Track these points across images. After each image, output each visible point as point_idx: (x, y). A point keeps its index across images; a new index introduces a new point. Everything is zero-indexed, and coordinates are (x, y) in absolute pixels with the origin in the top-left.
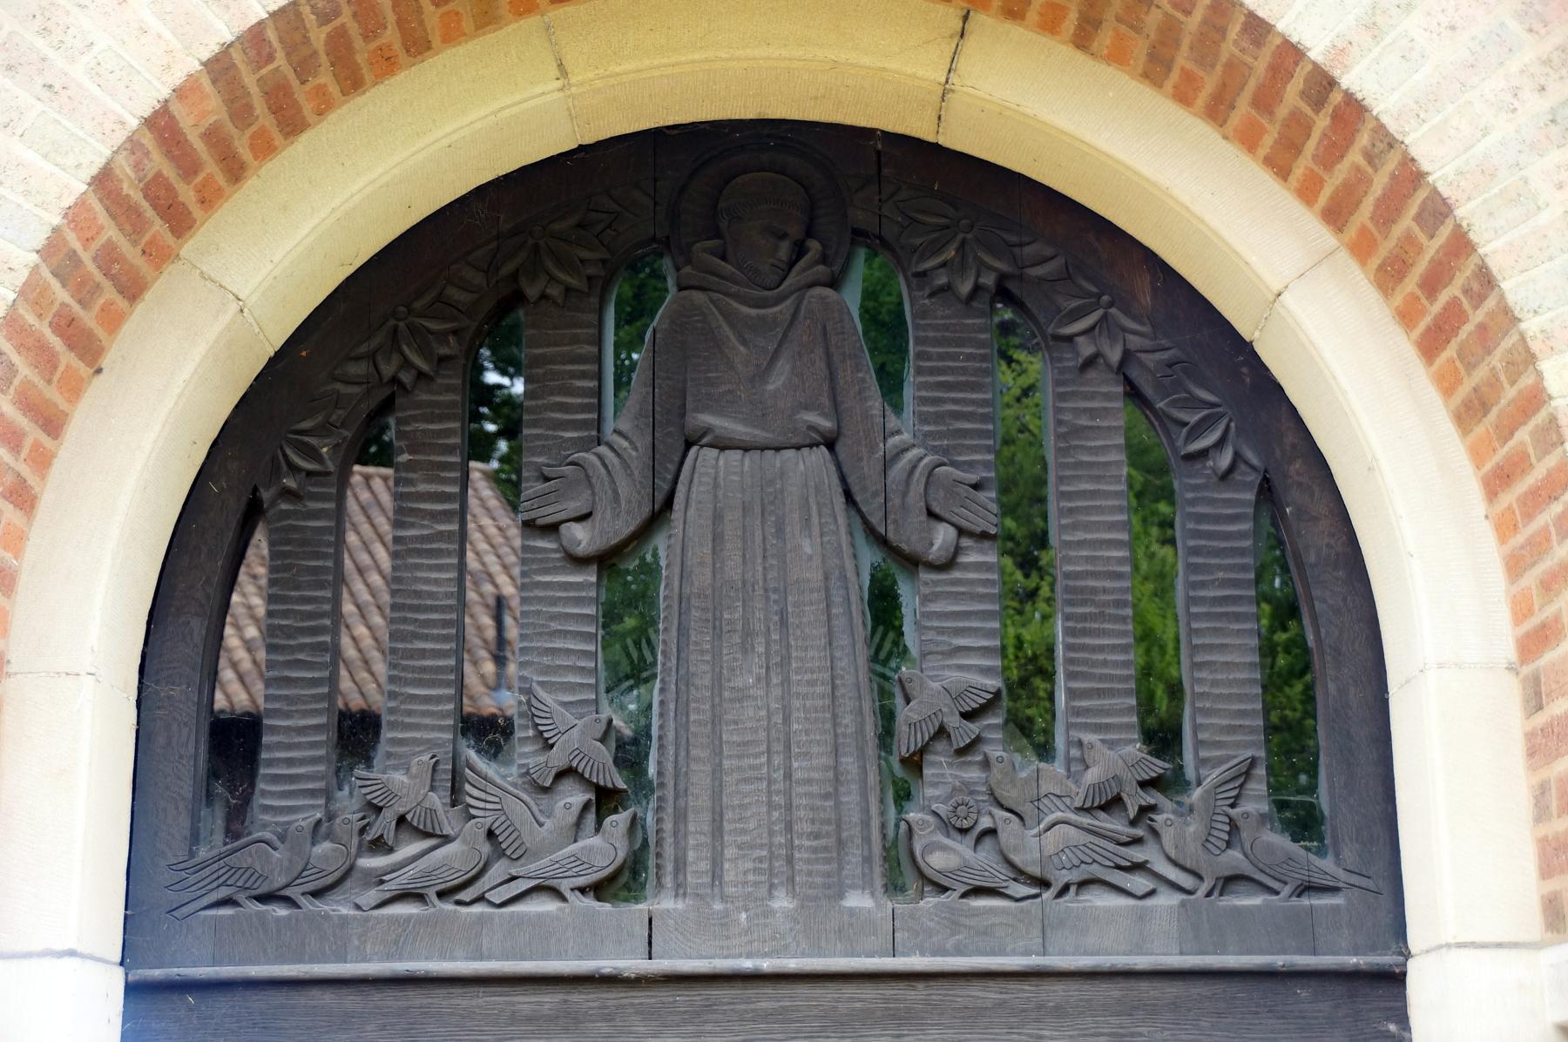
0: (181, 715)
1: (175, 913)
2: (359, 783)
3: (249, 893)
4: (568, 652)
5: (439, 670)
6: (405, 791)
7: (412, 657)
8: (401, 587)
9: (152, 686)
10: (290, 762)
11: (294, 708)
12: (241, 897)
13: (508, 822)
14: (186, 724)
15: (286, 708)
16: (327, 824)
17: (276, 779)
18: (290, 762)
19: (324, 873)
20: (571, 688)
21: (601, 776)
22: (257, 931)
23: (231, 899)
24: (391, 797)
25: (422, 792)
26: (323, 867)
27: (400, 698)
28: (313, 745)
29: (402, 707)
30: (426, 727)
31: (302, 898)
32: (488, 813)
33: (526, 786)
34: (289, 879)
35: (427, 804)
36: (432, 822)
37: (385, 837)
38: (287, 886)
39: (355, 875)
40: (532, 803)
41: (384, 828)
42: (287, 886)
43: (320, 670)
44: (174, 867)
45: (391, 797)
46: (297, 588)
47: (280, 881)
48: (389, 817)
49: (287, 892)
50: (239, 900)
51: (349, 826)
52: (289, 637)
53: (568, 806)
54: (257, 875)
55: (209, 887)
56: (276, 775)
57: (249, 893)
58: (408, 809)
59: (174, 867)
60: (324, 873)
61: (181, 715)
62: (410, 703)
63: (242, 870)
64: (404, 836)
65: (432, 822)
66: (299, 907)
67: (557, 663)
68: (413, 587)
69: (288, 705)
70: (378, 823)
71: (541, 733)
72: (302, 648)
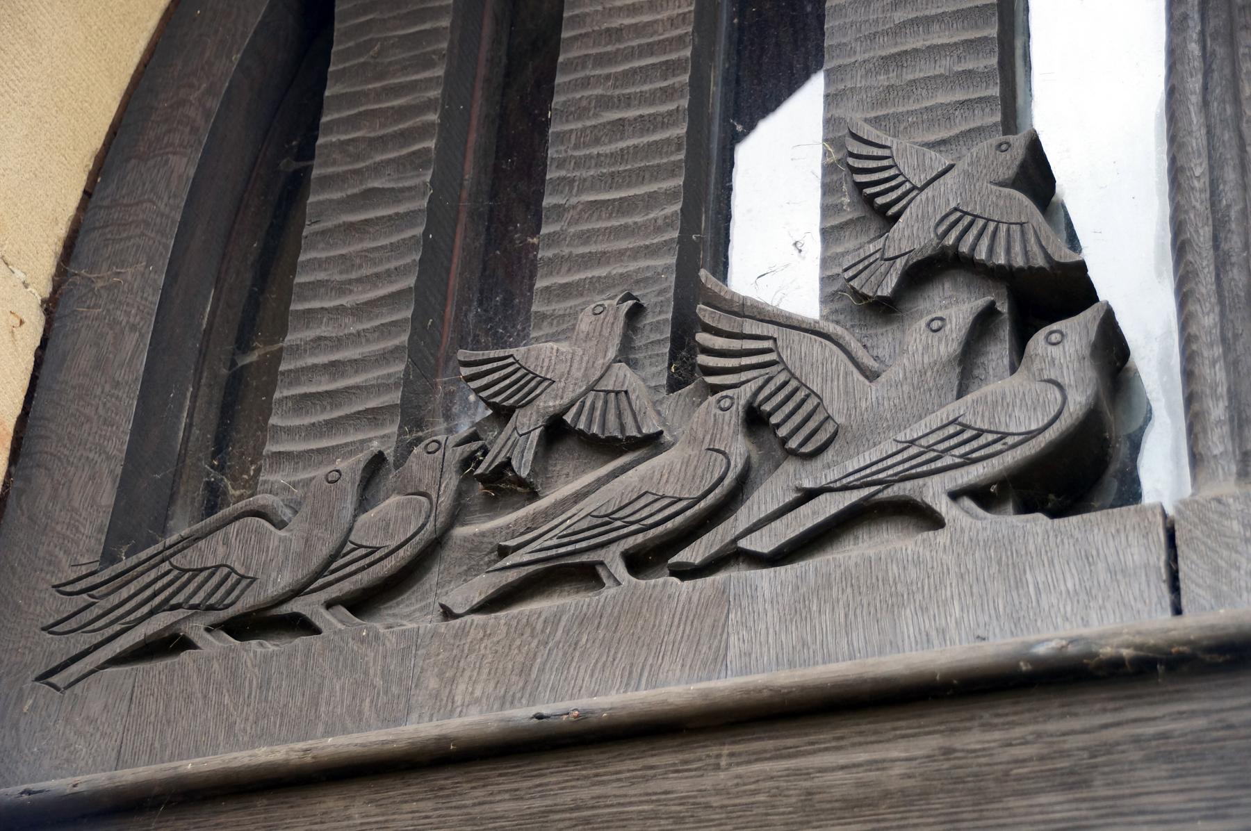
0: (128, 314)
1: (54, 679)
2: (465, 371)
3: (213, 617)
4: (935, 51)
5: (656, 148)
6: (562, 368)
7: (597, 141)
8: (583, 31)
9: (79, 271)
10: (335, 368)
11: (354, 275)
12: (195, 629)
13: (794, 383)
14: (133, 328)
15: (338, 277)
16: (394, 472)
17: (303, 402)
18: (335, 368)
19: (377, 555)
20: (945, 114)
21: (1017, 248)
22: (219, 691)
23: (175, 636)
24: (533, 384)
25: (600, 361)
26: (375, 543)
27: (568, 216)
28: (384, 331)
29: (572, 230)
30: (620, 255)
31: (327, 615)
32: (744, 376)
33: (841, 317)
34: (301, 574)
35: (608, 384)
36: (620, 415)
37: (514, 463)
38: (297, 592)
39: (450, 554)
40: (855, 346)
41: (514, 445)
42: (297, 592)
43: (412, 199)
44: (68, 589)
45: (533, 384)
46: (380, 77)
47: (281, 581)
48: (529, 423)
49: (297, 606)
50: (193, 636)
51: (439, 454)
52: (358, 158)
53: (935, 325)
54: (234, 577)
55: (139, 614)
56: (306, 396)
57: (213, 617)
58: (566, 400)
59: (68, 589)
60: (377, 555)
61: (128, 314)
62: (588, 220)
63: (205, 574)
64: (562, 463)
65: (620, 415)
66: (317, 631)
67: (910, 77)
68: (605, 25)
69: (341, 273)
70: (500, 441)
71: (870, 200)
72: (377, 169)
